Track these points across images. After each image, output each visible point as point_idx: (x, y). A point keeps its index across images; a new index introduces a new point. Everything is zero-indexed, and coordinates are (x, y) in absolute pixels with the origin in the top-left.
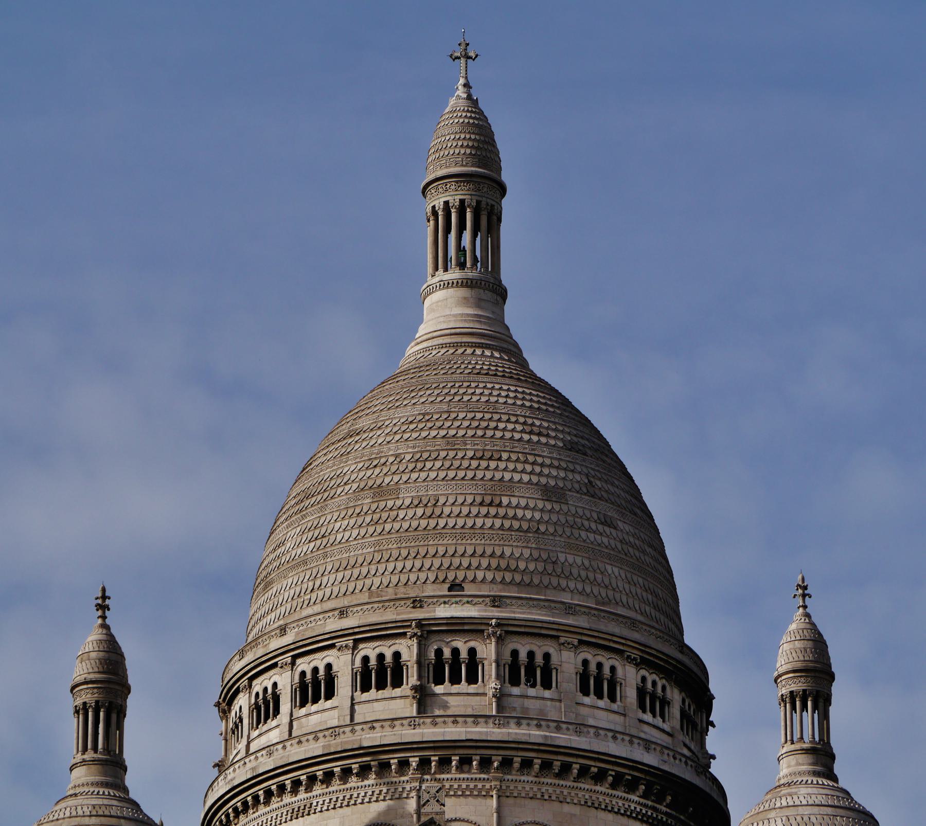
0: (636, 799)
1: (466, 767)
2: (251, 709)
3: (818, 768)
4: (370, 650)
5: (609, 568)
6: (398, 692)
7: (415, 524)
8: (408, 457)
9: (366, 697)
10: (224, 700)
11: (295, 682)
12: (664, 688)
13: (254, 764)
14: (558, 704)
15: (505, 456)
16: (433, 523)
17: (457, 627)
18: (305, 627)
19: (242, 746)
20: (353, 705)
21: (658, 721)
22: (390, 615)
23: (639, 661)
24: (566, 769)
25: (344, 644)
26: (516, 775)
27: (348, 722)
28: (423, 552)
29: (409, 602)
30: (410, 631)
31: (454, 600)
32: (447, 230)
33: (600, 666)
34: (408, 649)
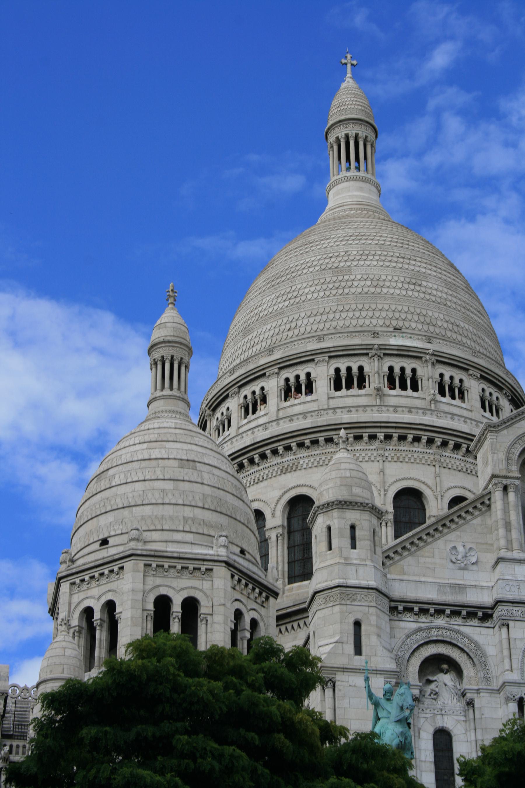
1: (416, 444)
2: (240, 407)
4: (343, 365)
5: (487, 340)
6: (362, 392)
8: (355, 253)
9: (338, 393)
10: (209, 408)
11: (280, 385)
14: (470, 413)
16: (378, 290)
18: (289, 349)
20: (329, 398)
22: (357, 341)
23: (510, 398)
25: (321, 359)
26: (450, 453)
29: (370, 334)
30: (372, 353)
33: (491, 394)
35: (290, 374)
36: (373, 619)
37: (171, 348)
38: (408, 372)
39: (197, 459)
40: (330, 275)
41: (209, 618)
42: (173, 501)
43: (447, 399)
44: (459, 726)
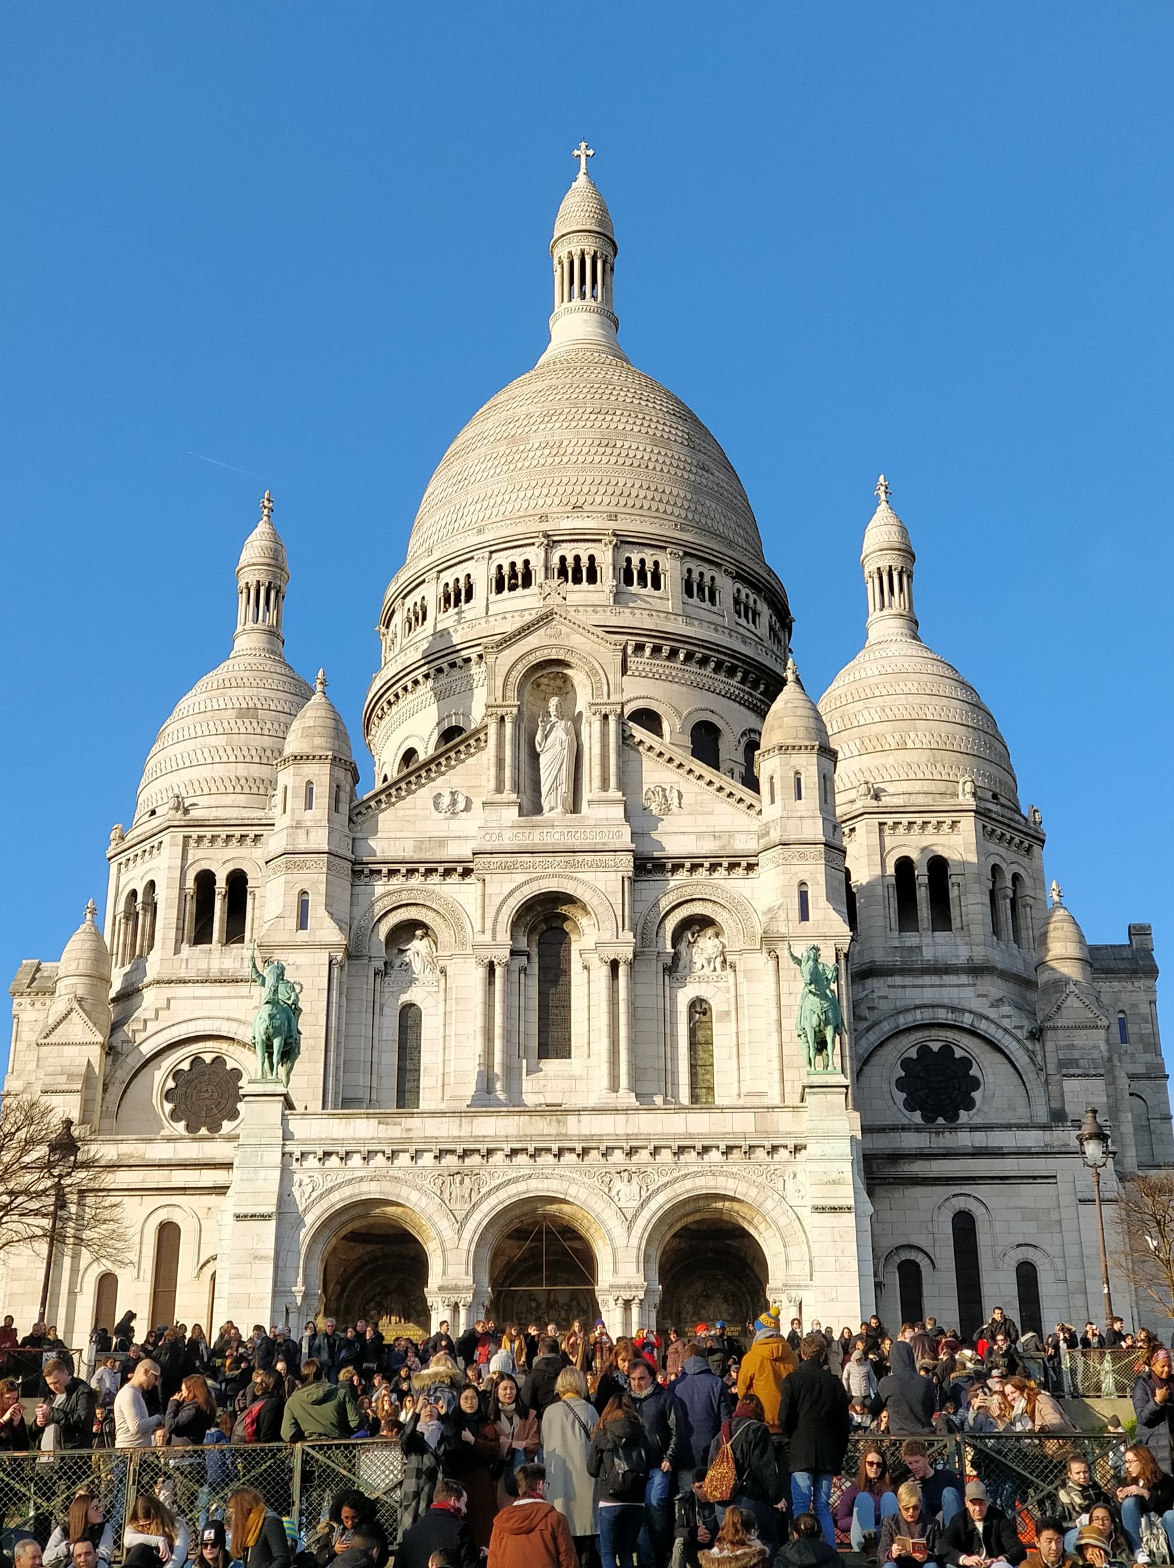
0: (735, 684)
3: (905, 631)
5: (708, 502)
6: (527, 591)
7: (542, 461)
13: (403, 659)
15: (619, 413)
16: (558, 460)
17: (578, 537)
21: (751, 626)
22: (520, 529)
24: (674, 653)
25: (481, 556)
27: (484, 615)
28: (549, 482)
29: (537, 518)
31: (575, 515)
32: (571, 282)
33: (701, 575)
34: (536, 557)
35: (448, 577)
36: (323, 887)
37: (256, 572)
38: (585, 562)
39: (260, 707)
40: (504, 447)
42: (224, 759)
43: (635, 588)
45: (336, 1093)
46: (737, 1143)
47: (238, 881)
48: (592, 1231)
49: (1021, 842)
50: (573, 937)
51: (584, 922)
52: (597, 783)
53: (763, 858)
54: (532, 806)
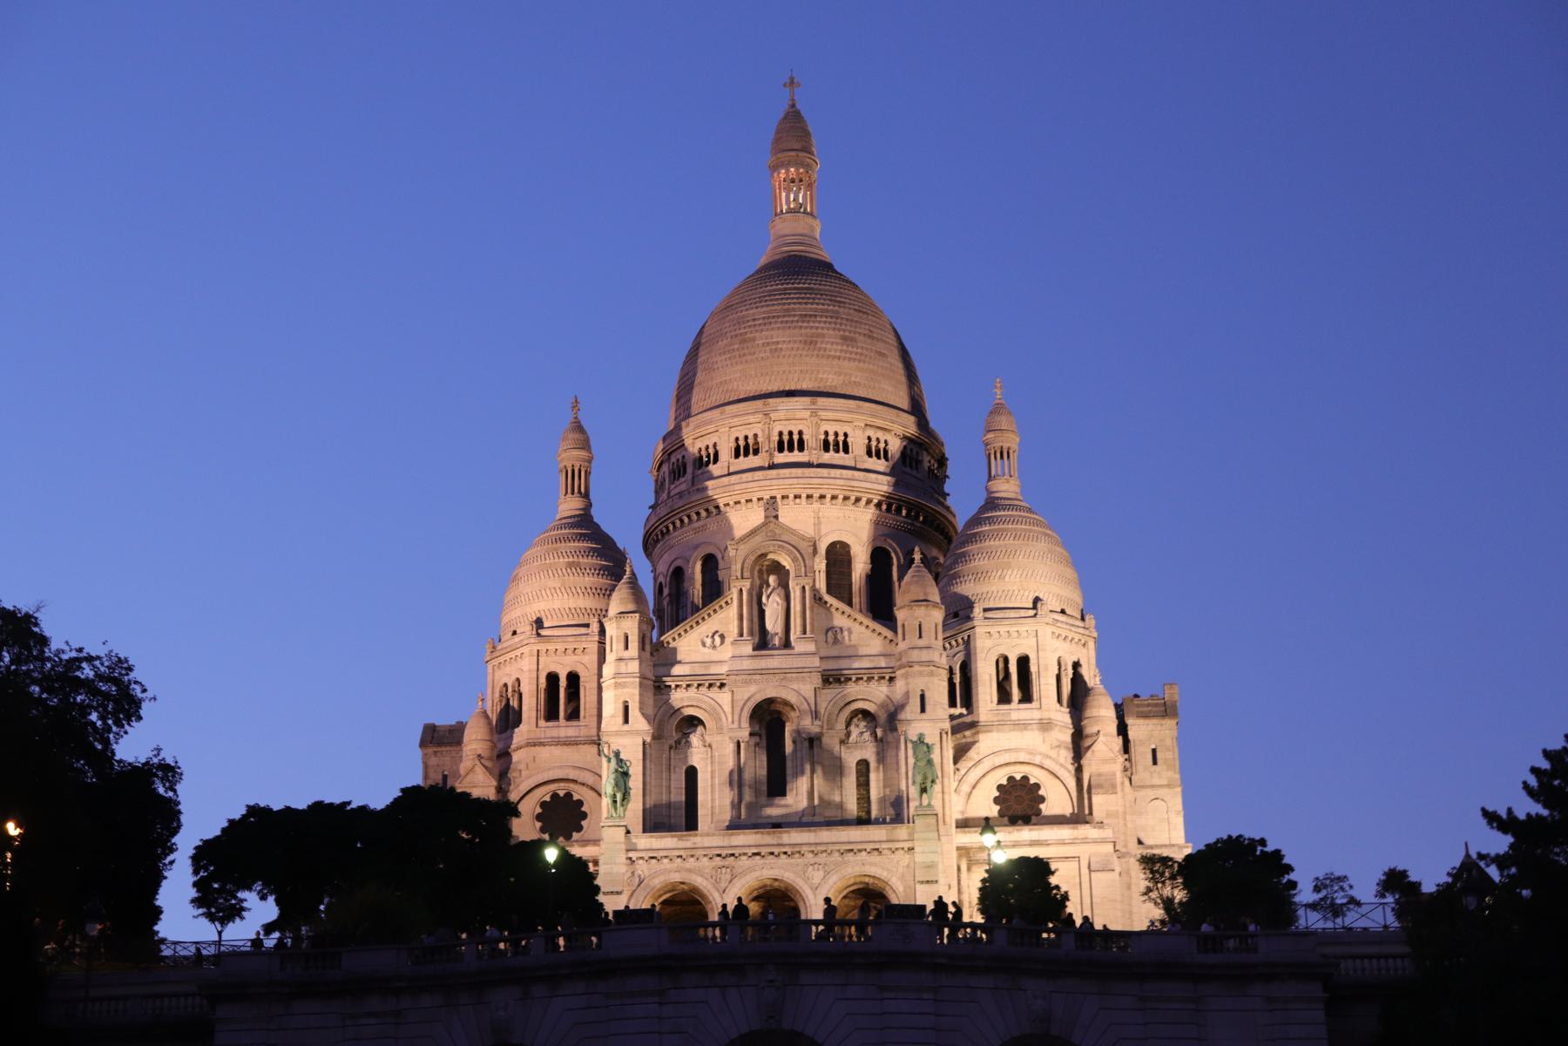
1: (798, 501)
12: (917, 453)
19: (665, 496)
21: (914, 472)
24: (858, 500)
33: (878, 440)
35: (701, 444)
36: (637, 698)
38: (796, 437)
41: (587, 685)
44: (702, 762)
45: (650, 820)
46: (876, 847)
47: (573, 678)
48: (798, 896)
49: (1080, 640)
50: (787, 724)
51: (793, 715)
52: (799, 629)
53: (899, 673)
54: (763, 642)
